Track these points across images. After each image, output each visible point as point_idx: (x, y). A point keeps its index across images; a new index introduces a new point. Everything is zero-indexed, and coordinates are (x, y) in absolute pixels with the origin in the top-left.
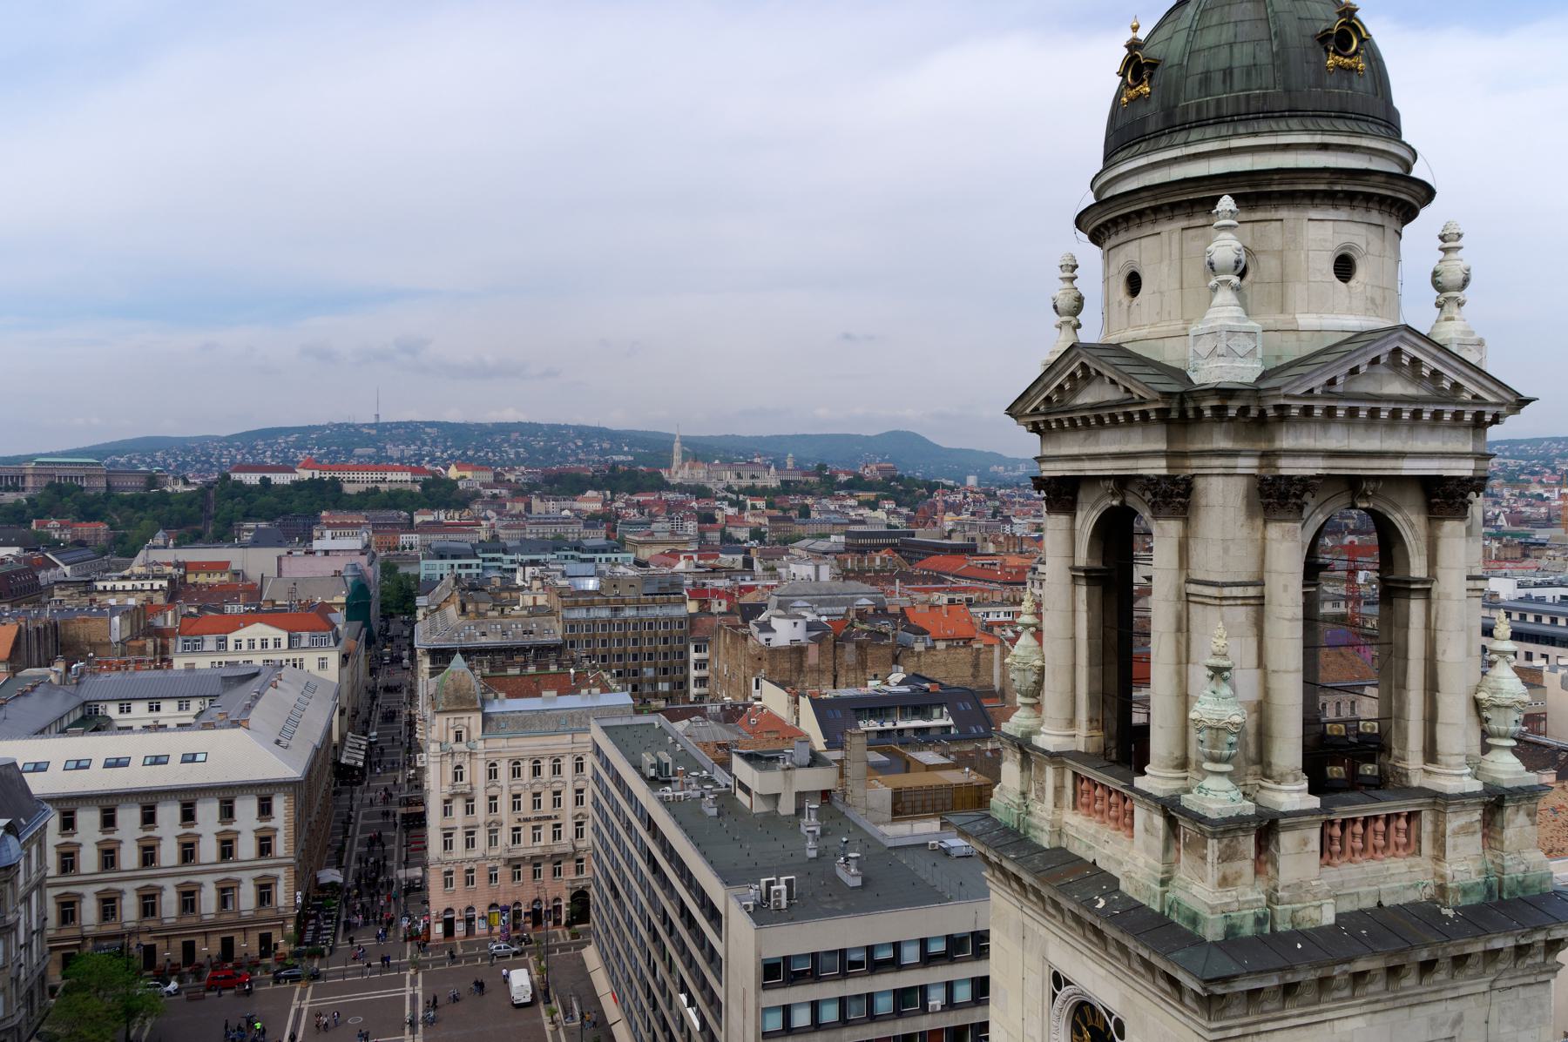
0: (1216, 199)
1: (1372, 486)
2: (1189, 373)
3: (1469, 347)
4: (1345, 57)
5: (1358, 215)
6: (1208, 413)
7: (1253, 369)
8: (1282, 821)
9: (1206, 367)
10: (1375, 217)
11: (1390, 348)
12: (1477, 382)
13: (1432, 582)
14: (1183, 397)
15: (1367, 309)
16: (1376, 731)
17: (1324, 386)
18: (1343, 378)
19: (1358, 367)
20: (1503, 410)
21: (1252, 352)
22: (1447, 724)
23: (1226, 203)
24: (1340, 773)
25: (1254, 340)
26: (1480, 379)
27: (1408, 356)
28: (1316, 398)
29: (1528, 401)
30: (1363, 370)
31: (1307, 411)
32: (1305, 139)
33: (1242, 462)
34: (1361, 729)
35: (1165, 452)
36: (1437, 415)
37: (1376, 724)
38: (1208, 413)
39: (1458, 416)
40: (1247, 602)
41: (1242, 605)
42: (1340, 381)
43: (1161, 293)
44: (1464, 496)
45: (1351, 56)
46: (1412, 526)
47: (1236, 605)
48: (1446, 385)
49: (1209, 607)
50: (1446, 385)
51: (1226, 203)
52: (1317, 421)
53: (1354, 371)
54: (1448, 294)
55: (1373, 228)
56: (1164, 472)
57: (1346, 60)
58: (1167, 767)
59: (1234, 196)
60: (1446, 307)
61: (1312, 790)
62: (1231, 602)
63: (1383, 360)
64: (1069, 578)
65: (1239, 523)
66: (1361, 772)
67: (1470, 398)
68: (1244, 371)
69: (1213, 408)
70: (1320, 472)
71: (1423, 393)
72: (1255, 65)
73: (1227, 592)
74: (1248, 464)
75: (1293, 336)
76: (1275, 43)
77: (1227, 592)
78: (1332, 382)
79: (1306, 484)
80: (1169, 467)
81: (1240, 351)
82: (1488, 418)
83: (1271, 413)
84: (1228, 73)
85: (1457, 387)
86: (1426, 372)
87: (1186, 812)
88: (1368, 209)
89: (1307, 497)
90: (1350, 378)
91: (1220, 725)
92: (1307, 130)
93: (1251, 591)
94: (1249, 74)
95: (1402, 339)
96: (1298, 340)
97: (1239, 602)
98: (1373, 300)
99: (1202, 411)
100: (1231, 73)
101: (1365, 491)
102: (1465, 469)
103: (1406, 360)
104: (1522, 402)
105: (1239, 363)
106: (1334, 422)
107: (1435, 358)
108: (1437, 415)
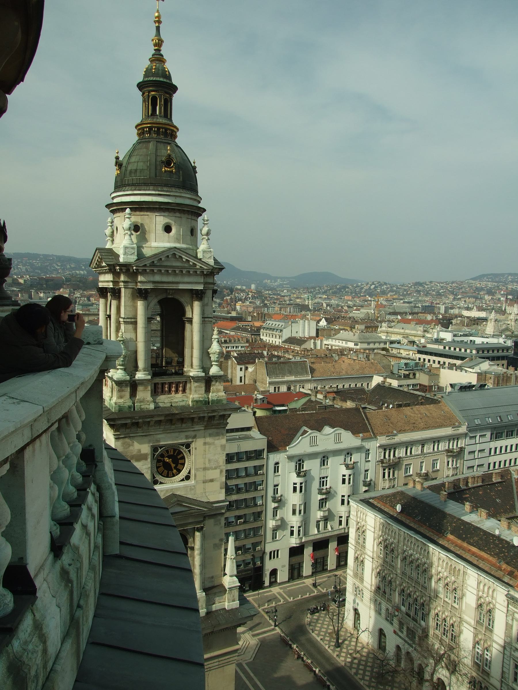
0: (126, 208)
4: (168, 168)
10: (178, 214)
11: (171, 253)
14: (114, 266)
23: (128, 211)
25: (134, 250)
30: (163, 259)
32: (153, 192)
42: (155, 262)
45: (170, 168)
48: (191, 263)
51: (128, 211)
55: (177, 218)
64: (105, 318)
68: (132, 258)
73: (125, 320)
75: (150, 249)
76: (148, 163)
78: (153, 262)
80: (113, 285)
82: (205, 273)
84: (136, 170)
85: (194, 263)
88: (175, 213)
94: (141, 171)
95: (175, 251)
103: (177, 257)
107: (186, 256)
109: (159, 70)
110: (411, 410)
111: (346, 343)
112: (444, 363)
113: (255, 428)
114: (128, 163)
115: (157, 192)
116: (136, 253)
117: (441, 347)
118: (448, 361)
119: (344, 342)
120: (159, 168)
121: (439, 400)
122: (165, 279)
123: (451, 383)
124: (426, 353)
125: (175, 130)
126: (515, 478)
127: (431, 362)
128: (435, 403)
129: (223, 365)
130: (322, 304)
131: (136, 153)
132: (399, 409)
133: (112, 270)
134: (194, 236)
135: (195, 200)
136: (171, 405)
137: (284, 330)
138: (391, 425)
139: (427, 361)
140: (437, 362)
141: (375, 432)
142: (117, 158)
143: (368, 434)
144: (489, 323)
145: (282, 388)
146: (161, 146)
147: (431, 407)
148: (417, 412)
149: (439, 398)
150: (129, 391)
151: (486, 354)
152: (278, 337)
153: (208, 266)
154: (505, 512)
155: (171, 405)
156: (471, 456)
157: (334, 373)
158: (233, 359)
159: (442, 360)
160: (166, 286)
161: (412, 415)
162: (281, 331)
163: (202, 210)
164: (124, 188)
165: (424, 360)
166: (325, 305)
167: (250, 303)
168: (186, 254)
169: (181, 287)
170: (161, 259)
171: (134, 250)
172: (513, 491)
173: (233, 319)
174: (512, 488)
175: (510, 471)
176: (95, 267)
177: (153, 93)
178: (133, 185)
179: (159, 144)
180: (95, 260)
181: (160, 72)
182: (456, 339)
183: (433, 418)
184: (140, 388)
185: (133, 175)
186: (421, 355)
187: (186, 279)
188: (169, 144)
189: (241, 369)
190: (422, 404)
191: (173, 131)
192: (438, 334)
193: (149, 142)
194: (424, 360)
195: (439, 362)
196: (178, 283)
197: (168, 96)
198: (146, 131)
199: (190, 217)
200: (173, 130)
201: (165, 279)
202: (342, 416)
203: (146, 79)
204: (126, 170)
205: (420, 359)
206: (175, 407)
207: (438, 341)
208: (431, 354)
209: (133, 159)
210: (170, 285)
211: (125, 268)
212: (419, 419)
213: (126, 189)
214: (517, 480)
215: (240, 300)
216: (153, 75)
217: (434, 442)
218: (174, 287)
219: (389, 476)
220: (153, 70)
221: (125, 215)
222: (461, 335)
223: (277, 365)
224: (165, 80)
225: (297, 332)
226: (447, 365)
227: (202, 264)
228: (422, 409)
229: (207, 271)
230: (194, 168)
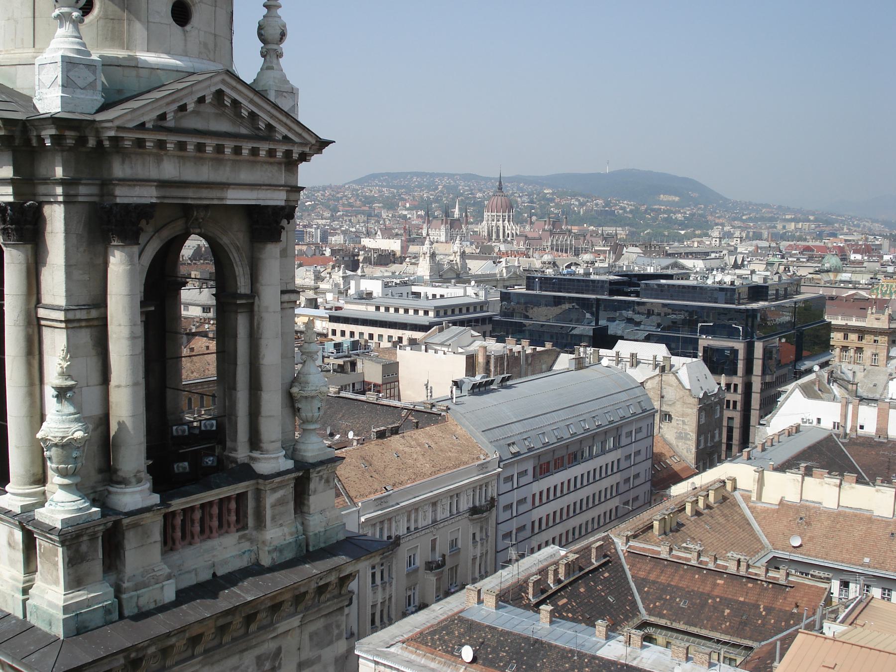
1: (202, 214)
2: (35, 101)
3: (285, 94)
6: (48, 143)
7: (92, 100)
8: (126, 521)
9: (49, 96)
11: (214, 89)
12: (286, 124)
15: (200, 53)
16: (214, 428)
17: (154, 120)
18: (173, 114)
19: (185, 105)
20: (307, 150)
21: (92, 86)
22: (266, 417)
24: (185, 468)
25: (94, 73)
26: (289, 122)
27: (229, 98)
28: (148, 130)
29: (327, 143)
30: (191, 107)
31: (140, 143)
33: (82, 190)
34: (203, 428)
35: (11, 179)
36: (254, 152)
37: (214, 422)
38: (48, 143)
39: (271, 153)
40: (91, 323)
41: (87, 327)
42: (170, 116)
43: (16, 21)
44: (278, 223)
46: (238, 249)
47: (81, 327)
49: (56, 330)
50: (262, 125)
52: (150, 154)
53: (183, 108)
54: (270, 46)
56: (11, 199)
58: (25, 484)
60: (268, 57)
61: (155, 490)
63: (208, 100)
65: (81, 249)
66: (204, 464)
67: (280, 138)
69: (52, 136)
70: (154, 201)
71: (244, 131)
74: (85, 192)
75: (134, 72)
78: (163, 117)
79: (144, 212)
80: (15, 194)
81: (80, 83)
82: (295, 156)
83: (107, 143)
85: (270, 127)
86: (245, 113)
87: (39, 525)
89: (143, 223)
90: (180, 114)
93: (94, 313)
95: (223, 82)
97: (83, 324)
98: (205, 45)
99: (43, 140)
101: (197, 219)
102: (277, 198)
103: (228, 102)
104: (322, 144)
105: (79, 94)
106: (165, 154)
107: (252, 101)
108: (254, 152)
110: (402, 441)
112: (400, 339)
116: (99, 88)
117: (373, 309)
118: (407, 334)
121: (443, 414)
123: (454, 380)
126: (622, 550)
128: (436, 422)
132: (381, 441)
133: (17, 142)
136: (214, 575)
138: (374, 474)
140: (385, 338)
141: (352, 494)
144: (421, 259)
147: (431, 429)
148: (413, 443)
149: (443, 410)
150: (101, 556)
153: (305, 135)
154: (627, 618)
155: (214, 575)
156: (507, 515)
157: (192, 373)
159: (396, 333)
160: (192, 197)
161: (407, 449)
168: (251, 95)
169: (236, 197)
170: (183, 108)
171: (94, 73)
172: (626, 575)
174: (623, 570)
175: (611, 538)
183: (441, 450)
186: (336, 324)
187: (245, 175)
190: (417, 426)
194: (380, 336)
195: (390, 337)
196: (225, 186)
201: (190, 173)
205: (371, 336)
206: (223, 577)
210: (205, 193)
211: (72, 133)
212: (420, 457)
214: (626, 554)
217: (451, 497)
218: (209, 197)
219: (382, 579)
222: (396, 284)
226: (405, 342)
227: (290, 129)
228: (421, 435)
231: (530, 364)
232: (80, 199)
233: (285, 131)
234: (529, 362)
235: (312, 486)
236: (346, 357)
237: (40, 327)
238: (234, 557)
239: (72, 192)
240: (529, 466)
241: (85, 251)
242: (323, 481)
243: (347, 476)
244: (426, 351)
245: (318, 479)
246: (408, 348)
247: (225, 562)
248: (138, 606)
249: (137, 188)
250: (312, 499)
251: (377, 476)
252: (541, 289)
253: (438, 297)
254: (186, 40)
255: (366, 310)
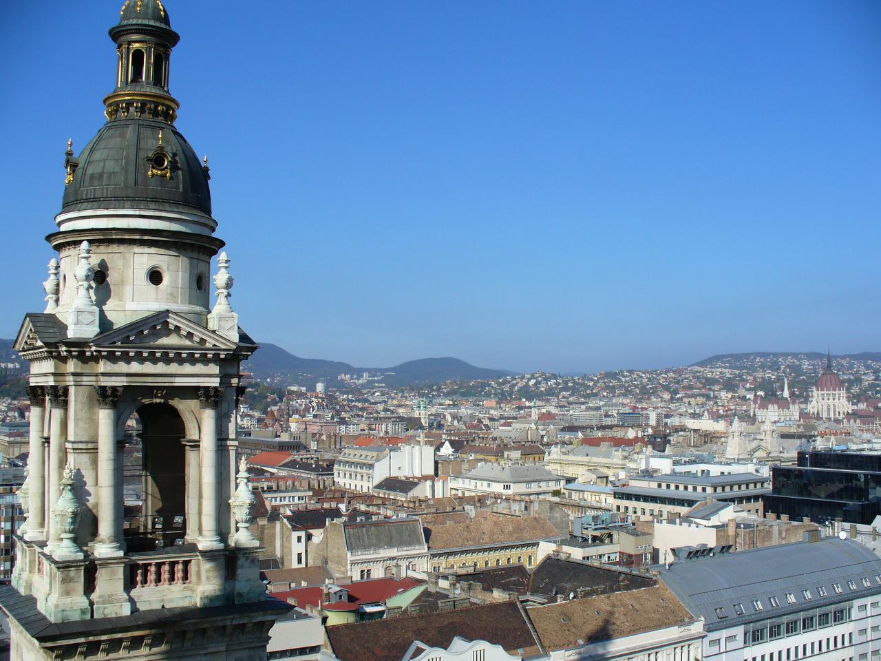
0: (81, 242)
5: (162, 251)
13: (200, 441)
14: (56, 345)
15: (168, 299)
23: (85, 245)
25: (94, 316)
45: (161, 170)
57: (159, 172)
59: (88, 240)
62: (79, 451)
64: (40, 444)
68: (90, 331)
70: (125, 384)
72: (113, 172)
73: (76, 446)
75: (123, 313)
77: (76, 446)
80: (55, 381)
82: (222, 356)
84: (101, 175)
91: (63, 513)
92: (132, 208)
94: (110, 176)
96: (125, 315)
97: (84, 451)
100: (103, 176)
105: (85, 328)
107: (188, 326)
109: (147, 7)
110: (607, 601)
111: (489, 485)
113: (326, 648)
114: (89, 163)
115: (138, 212)
117: (654, 485)
118: (667, 509)
119: (485, 483)
120: (142, 169)
121: (655, 578)
122: (148, 368)
124: (628, 497)
125: (173, 105)
127: (639, 513)
129: (266, 531)
130: (444, 416)
131: (102, 145)
134: (203, 291)
135: (205, 225)
136: (163, 607)
137: (377, 465)
139: (631, 510)
140: (647, 512)
141: (546, 643)
142: (69, 154)
143: (533, 648)
145: (376, 571)
146: (146, 132)
150: (82, 580)
151: (728, 493)
152: (365, 477)
155: (163, 607)
157: (468, 541)
158: (285, 520)
159: (656, 507)
160: (150, 382)
162: (371, 466)
163: (218, 243)
164: (80, 205)
165: (627, 508)
166: (449, 418)
167: (315, 416)
168: (187, 323)
171: (94, 316)
173: (284, 447)
176: (23, 348)
177: (137, 45)
178: (95, 200)
179: (143, 130)
180: (24, 335)
181: (150, 10)
182: (679, 469)
183: (645, 612)
184: (102, 576)
185: (96, 183)
188: (161, 128)
189: (299, 539)
191: (169, 107)
192: (647, 463)
193: (127, 126)
194: (627, 508)
197: (162, 49)
198: (122, 108)
199: (195, 255)
200: (170, 106)
202: (485, 618)
203: (125, 22)
204: (84, 174)
205: (618, 507)
207: (648, 474)
208: (638, 497)
209: (97, 155)
213: (83, 208)
215: (296, 411)
216: (138, 16)
220: (138, 8)
221: (78, 252)
223: (364, 530)
224: (158, 24)
225: (400, 468)
226: (665, 516)
227: (217, 341)
229: (226, 352)
230: (206, 170)
231: (785, 538)
232: (84, 383)
233: (214, 342)
234: (783, 536)
235: (240, 563)
236: (604, 528)
237: (67, 452)
238: (178, 598)
239: (79, 380)
240: (739, 631)
241: (86, 412)
242: (249, 561)
243: (545, 628)
244: (681, 524)
245: (244, 558)
246: (664, 522)
247: (171, 601)
248: (104, 614)
249: (114, 377)
250: (239, 571)
251: (574, 630)
252: (811, 466)
253: (726, 474)
254: (157, 293)
255: (649, 486)
